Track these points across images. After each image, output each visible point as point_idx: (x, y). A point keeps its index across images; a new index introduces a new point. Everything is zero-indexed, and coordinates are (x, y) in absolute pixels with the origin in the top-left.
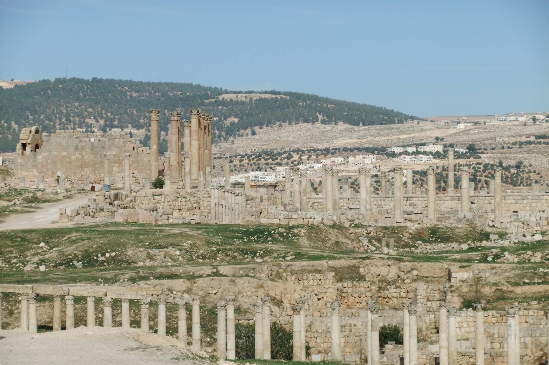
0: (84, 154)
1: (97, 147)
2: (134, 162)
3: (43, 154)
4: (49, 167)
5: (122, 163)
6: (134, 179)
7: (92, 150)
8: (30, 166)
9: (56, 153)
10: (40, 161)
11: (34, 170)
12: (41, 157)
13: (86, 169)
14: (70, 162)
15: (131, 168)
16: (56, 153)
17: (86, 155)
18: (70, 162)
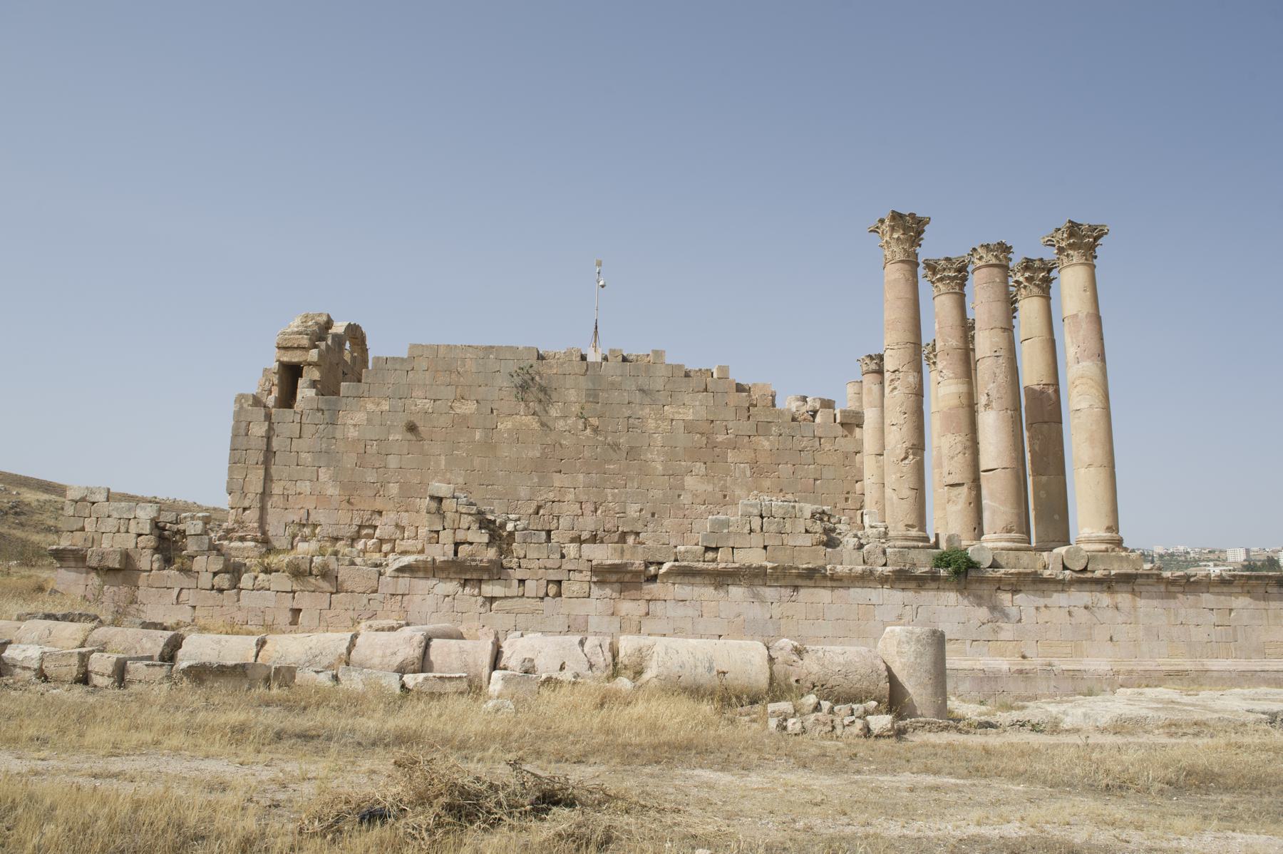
3: (370, 406)
4: (393, 462)
6: (818, 527)
7: (593, 396)
8: (306, 458)
9: (429, 405)
10: (353, 433)
11: (324, 475)
12: (360, 417)
13: (558, 480)
14: (489, 446)
15: (767, 483)
16: (429, 405)
17: (565, 417)
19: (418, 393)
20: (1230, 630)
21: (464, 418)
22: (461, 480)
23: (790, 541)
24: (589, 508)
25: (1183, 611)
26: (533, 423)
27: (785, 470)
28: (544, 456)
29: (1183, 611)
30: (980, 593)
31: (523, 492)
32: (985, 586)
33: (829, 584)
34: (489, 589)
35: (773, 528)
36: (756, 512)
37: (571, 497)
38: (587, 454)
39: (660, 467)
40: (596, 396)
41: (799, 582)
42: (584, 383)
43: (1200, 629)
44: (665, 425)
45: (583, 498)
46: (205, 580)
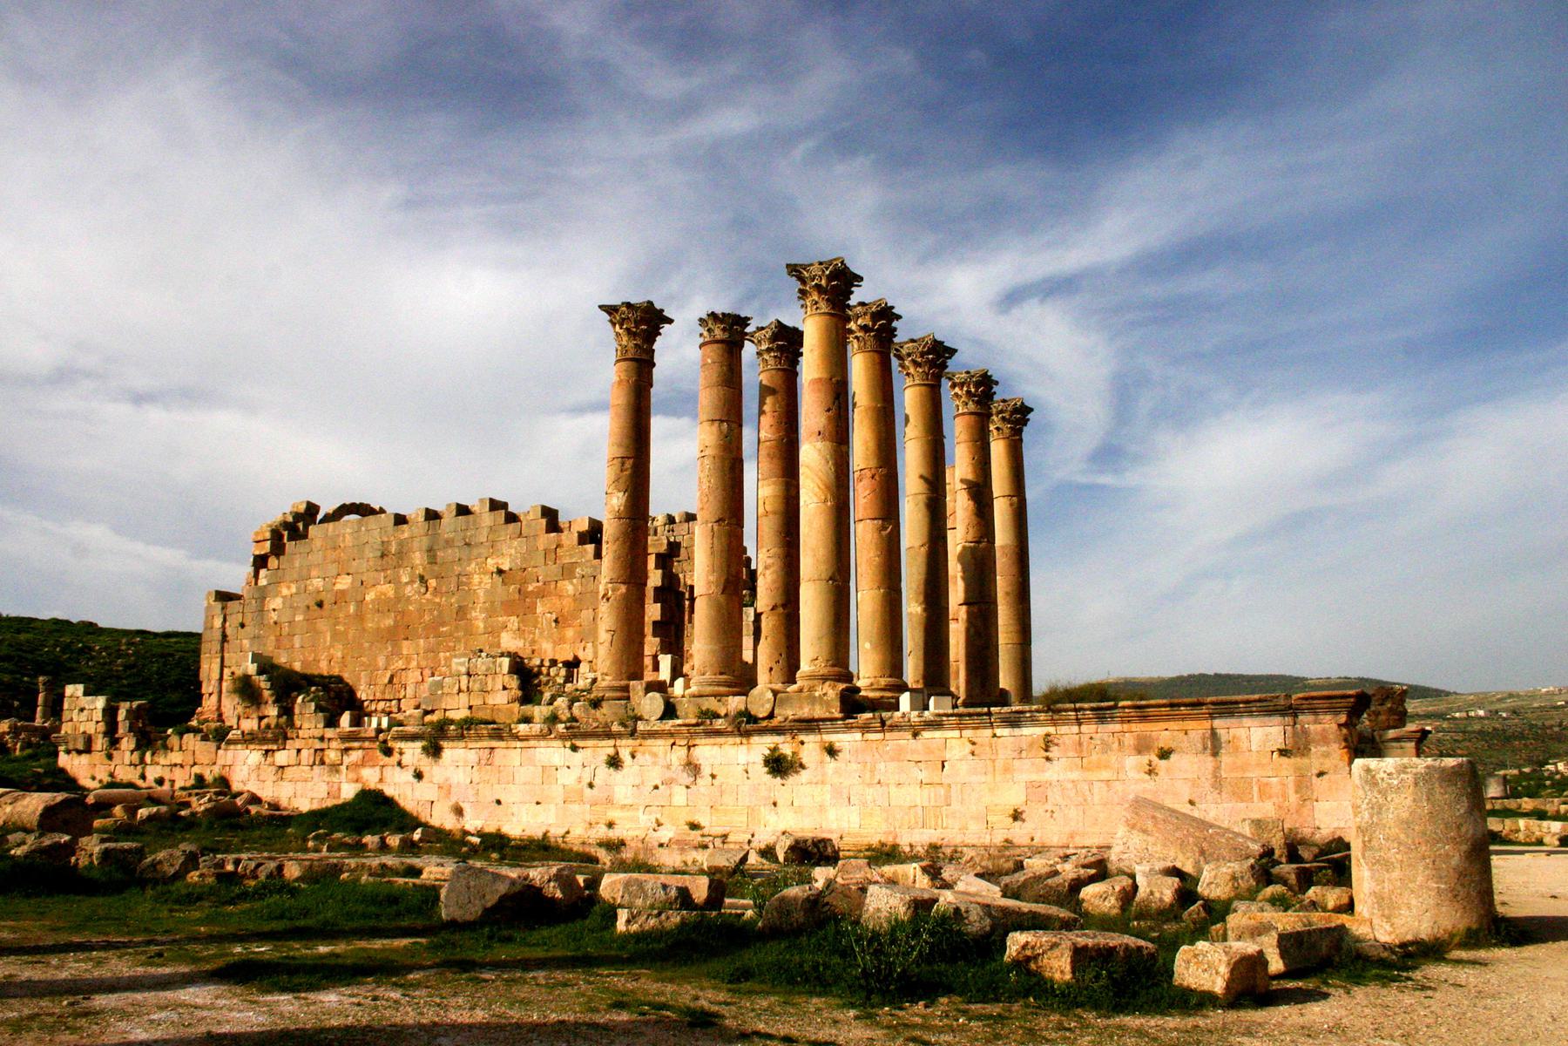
0: (405, 579)
1: (449, 543)
2: (579, 598)
4: (297, 642)
5: (532, 608)
9: (317, 583)
10: (274, 616)
13: (406, 647)
14: (360, 616)
17: (412, 582)
18: (360, 616)
19: (314, 573)
20: (942, 791)
21: (343, 592)
22: (339, 654)
23: (490, 701)
24: (427, 672)
25: (882, 766)
26: (389, 590)
27: (586, 614)
28: (396, 626)
29: (882, 766)
30: (655, 749)
31: (381, 661)
32: (660, 742)
33: (519, 744)
34: (281, 757)
35: (476, 687)
36: (464, 670)
37: (414, 664)
38: (427, 618)
39: (481, 625)
40: (435, 556)
41: (494, 744)
42: (425, 542)
43: (903, 790)
44: (487, 579)
45: (423, 664)
46: (127, 758)
